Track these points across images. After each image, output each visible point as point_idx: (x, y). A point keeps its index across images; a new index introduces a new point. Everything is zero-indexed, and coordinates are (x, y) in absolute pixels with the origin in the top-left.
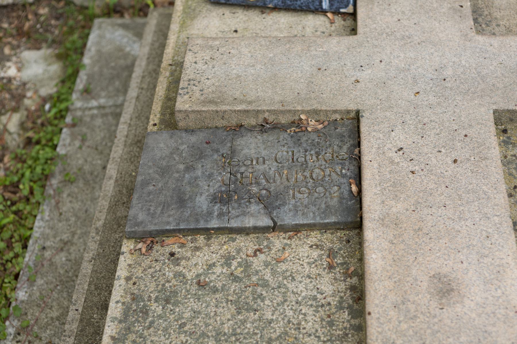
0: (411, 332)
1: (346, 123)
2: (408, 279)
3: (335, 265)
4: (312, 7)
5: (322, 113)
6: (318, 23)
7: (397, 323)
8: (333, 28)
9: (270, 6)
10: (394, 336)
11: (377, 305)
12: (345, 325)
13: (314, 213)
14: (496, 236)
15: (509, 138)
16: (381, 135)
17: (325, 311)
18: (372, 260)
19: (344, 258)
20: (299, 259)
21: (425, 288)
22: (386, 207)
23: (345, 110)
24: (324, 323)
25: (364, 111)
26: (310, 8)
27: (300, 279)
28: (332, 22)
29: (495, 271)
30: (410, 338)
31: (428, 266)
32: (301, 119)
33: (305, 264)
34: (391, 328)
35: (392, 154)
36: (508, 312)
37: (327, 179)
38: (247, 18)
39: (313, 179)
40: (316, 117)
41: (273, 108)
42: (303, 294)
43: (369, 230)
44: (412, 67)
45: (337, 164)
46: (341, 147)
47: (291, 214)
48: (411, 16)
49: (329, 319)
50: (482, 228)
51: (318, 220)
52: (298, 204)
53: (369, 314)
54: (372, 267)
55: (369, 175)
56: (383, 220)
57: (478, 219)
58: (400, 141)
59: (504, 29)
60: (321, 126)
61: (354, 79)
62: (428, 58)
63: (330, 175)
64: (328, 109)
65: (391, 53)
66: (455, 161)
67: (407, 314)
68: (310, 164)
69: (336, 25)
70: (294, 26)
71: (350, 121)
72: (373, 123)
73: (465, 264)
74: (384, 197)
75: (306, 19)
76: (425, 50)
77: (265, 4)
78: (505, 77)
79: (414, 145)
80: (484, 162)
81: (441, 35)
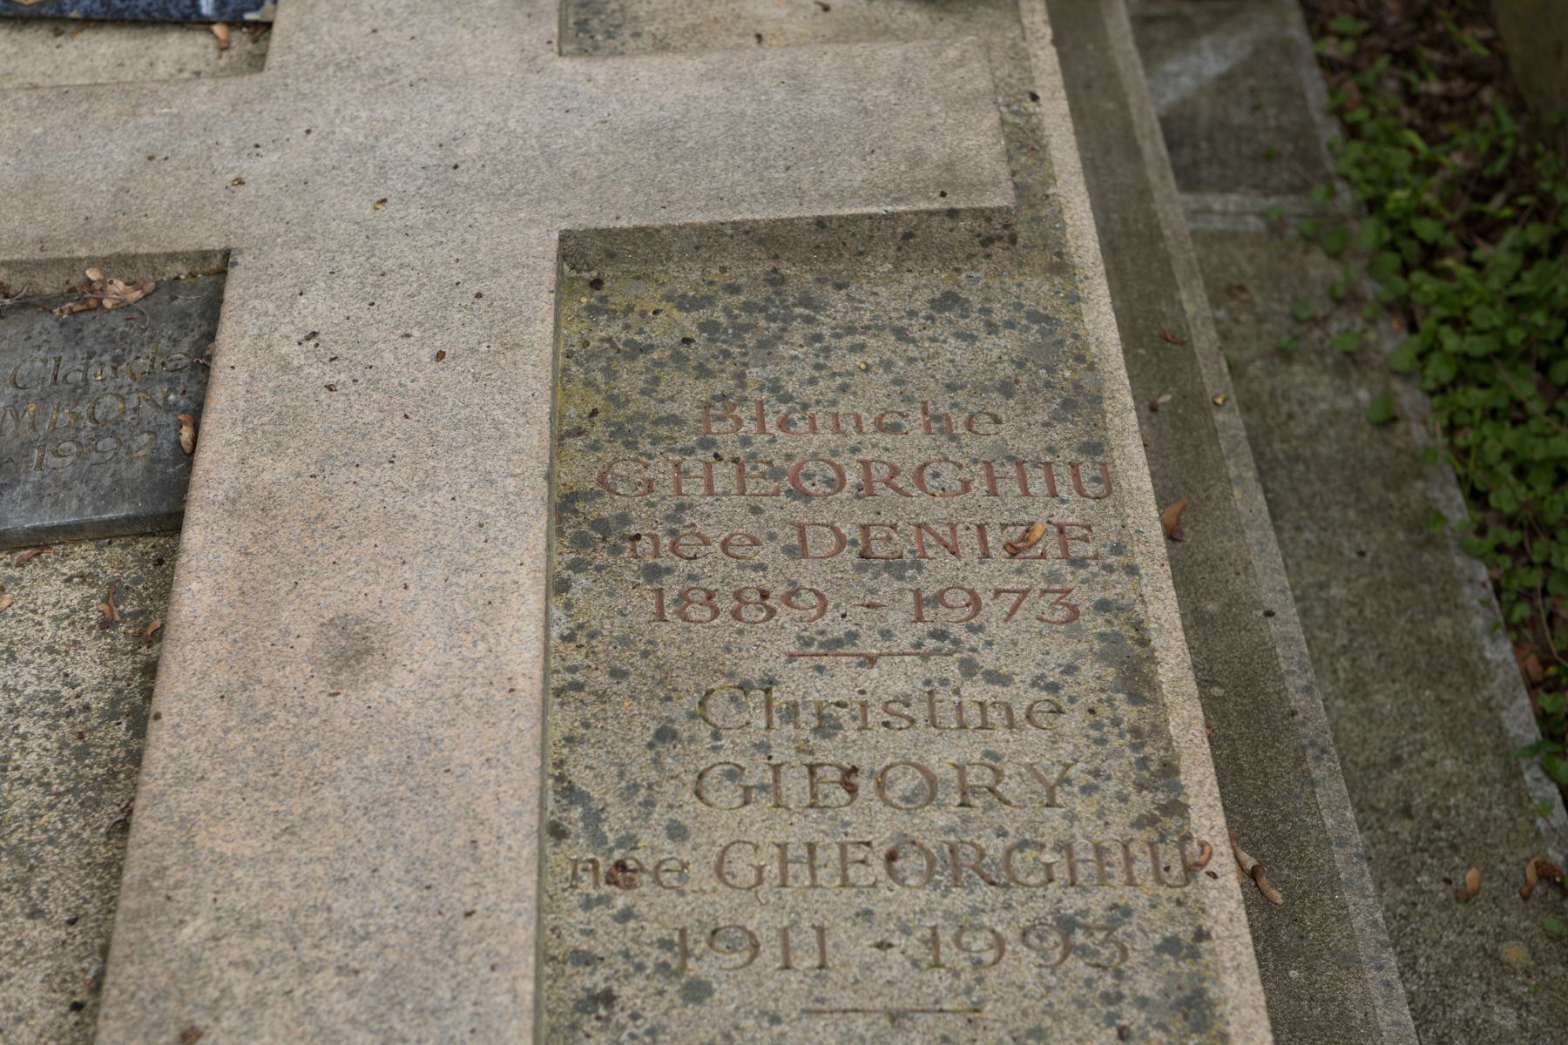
0: (249, 750)
1: (201, 285)
2: (267, 633)
3: (117, 618)
4: (173, 12)
5: (139, 264)
6: (189, 50)
7: (220, 734)
8: (222, 62)
9: (74, 14)
10: (206, 764)
11: (179, 698)
12: (115, 753)
13: (81, 500)
14: (502, 522)
15: (604, 299)
16: (271, 306)
17: (74, 725)
18: (189, 594)
19: (141, 599)
20: (34, 611)
21: (304, 650)
22: (249, 471)
23: (195, 252)
24: (66, 752)
25: (241, 252)
26: (170, 15)
27: (28, 657)
28: (224, 47)
29: (481, 602)
30: (243, 766)
31: (322, 600)
32: (90, 282)
33: (46, 622)
34: (203, 747)
35: (290, 349)
36: (493, 691)
37: (128, 419)
38: (15, 49)
39: (96, 421)
40: (127, 272)
41: (16, 257)
42: (29, 691)
43: (196, 528)
44: (384, 140)
45: (161, 381)
46: (175, 342)
47: (27, 504)
48: (407, 20)
49: (80, 743)
50: (472, 504)
51: (89, 515)
52: (48, 480)
53: (158, 717)
54: (185, 611)
55: (223, 399)
56: (234, 502)
57: (465, 487)
58: (316, 318)
59: (651, 41)
60: (138, 294)
61: (231, 177)
62: (427, 117)
63: (135, 410)
64: (154, 250)
65: (338, 111)
66: (440, 356)
67: (250, 711)
68: (94, 386)
69: (233, 52)
70: (128, 63)
71: (212, 279)
72: (256, 279)
73: (413, 590)
74: (248, 450)
75: (162, 43)
76: (422, 100)
77: (60, 10)
78: (606, 154)
79: (349, 323)
80: (509, 354)
81: (470, 62)
